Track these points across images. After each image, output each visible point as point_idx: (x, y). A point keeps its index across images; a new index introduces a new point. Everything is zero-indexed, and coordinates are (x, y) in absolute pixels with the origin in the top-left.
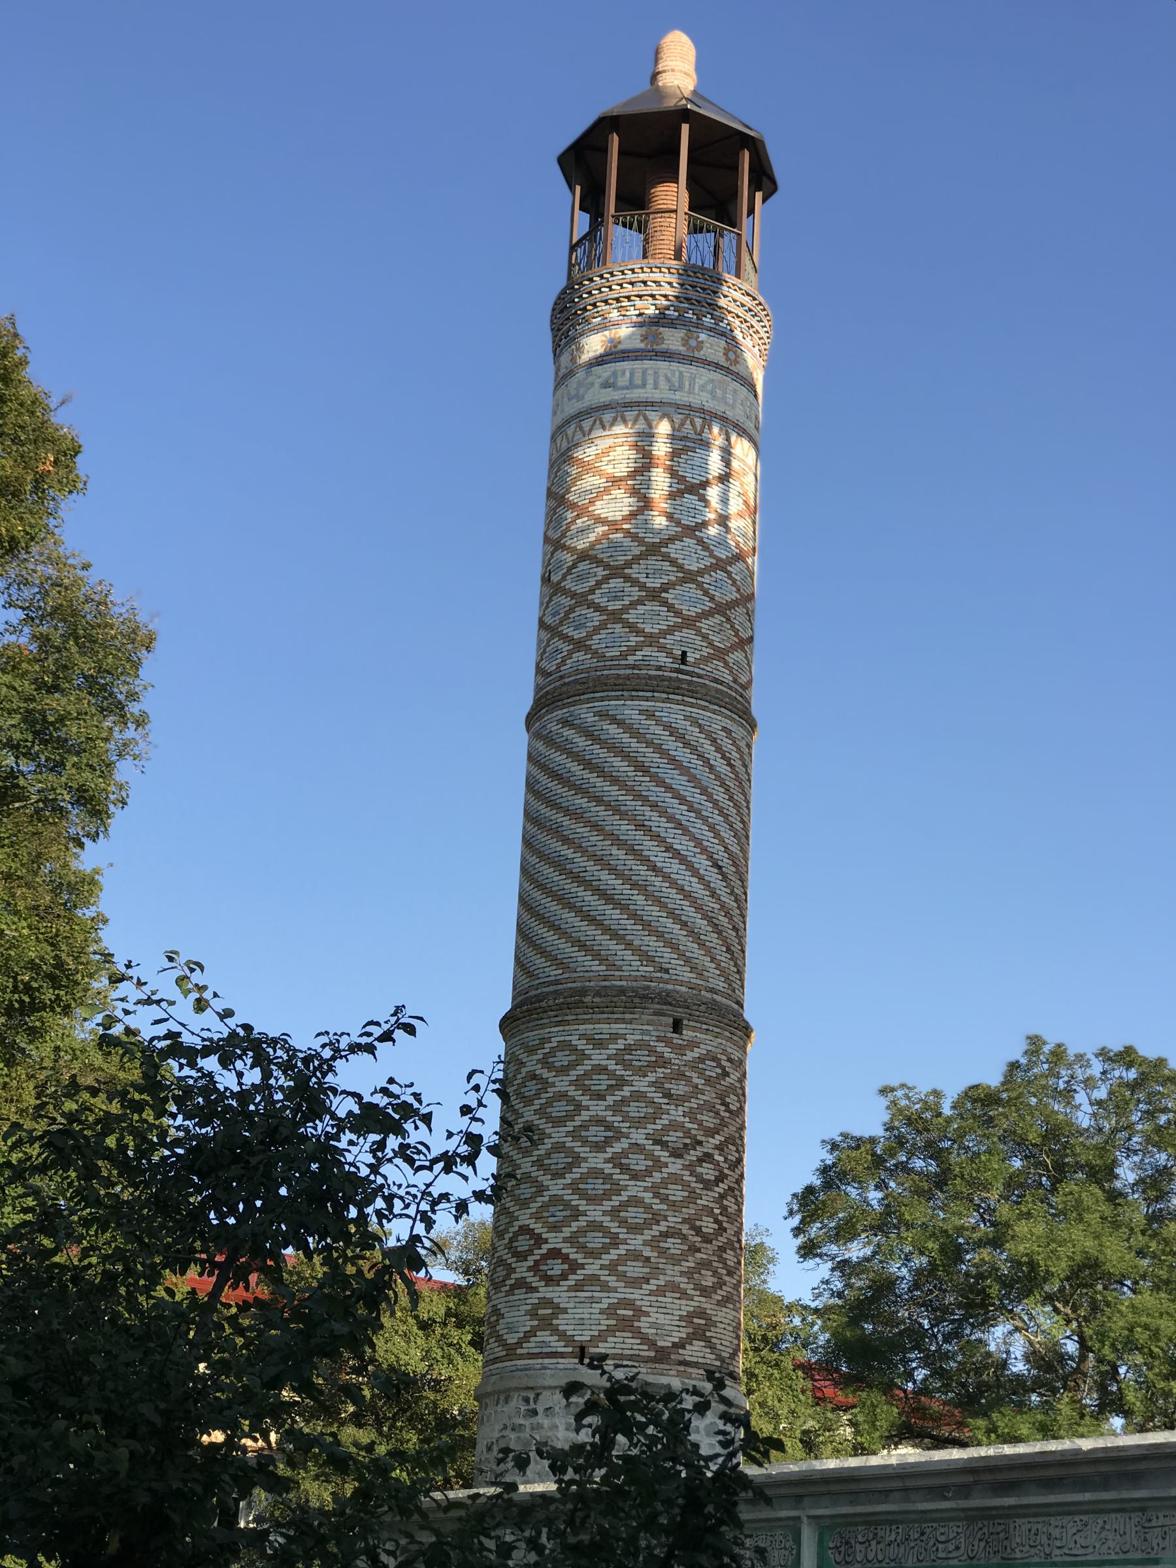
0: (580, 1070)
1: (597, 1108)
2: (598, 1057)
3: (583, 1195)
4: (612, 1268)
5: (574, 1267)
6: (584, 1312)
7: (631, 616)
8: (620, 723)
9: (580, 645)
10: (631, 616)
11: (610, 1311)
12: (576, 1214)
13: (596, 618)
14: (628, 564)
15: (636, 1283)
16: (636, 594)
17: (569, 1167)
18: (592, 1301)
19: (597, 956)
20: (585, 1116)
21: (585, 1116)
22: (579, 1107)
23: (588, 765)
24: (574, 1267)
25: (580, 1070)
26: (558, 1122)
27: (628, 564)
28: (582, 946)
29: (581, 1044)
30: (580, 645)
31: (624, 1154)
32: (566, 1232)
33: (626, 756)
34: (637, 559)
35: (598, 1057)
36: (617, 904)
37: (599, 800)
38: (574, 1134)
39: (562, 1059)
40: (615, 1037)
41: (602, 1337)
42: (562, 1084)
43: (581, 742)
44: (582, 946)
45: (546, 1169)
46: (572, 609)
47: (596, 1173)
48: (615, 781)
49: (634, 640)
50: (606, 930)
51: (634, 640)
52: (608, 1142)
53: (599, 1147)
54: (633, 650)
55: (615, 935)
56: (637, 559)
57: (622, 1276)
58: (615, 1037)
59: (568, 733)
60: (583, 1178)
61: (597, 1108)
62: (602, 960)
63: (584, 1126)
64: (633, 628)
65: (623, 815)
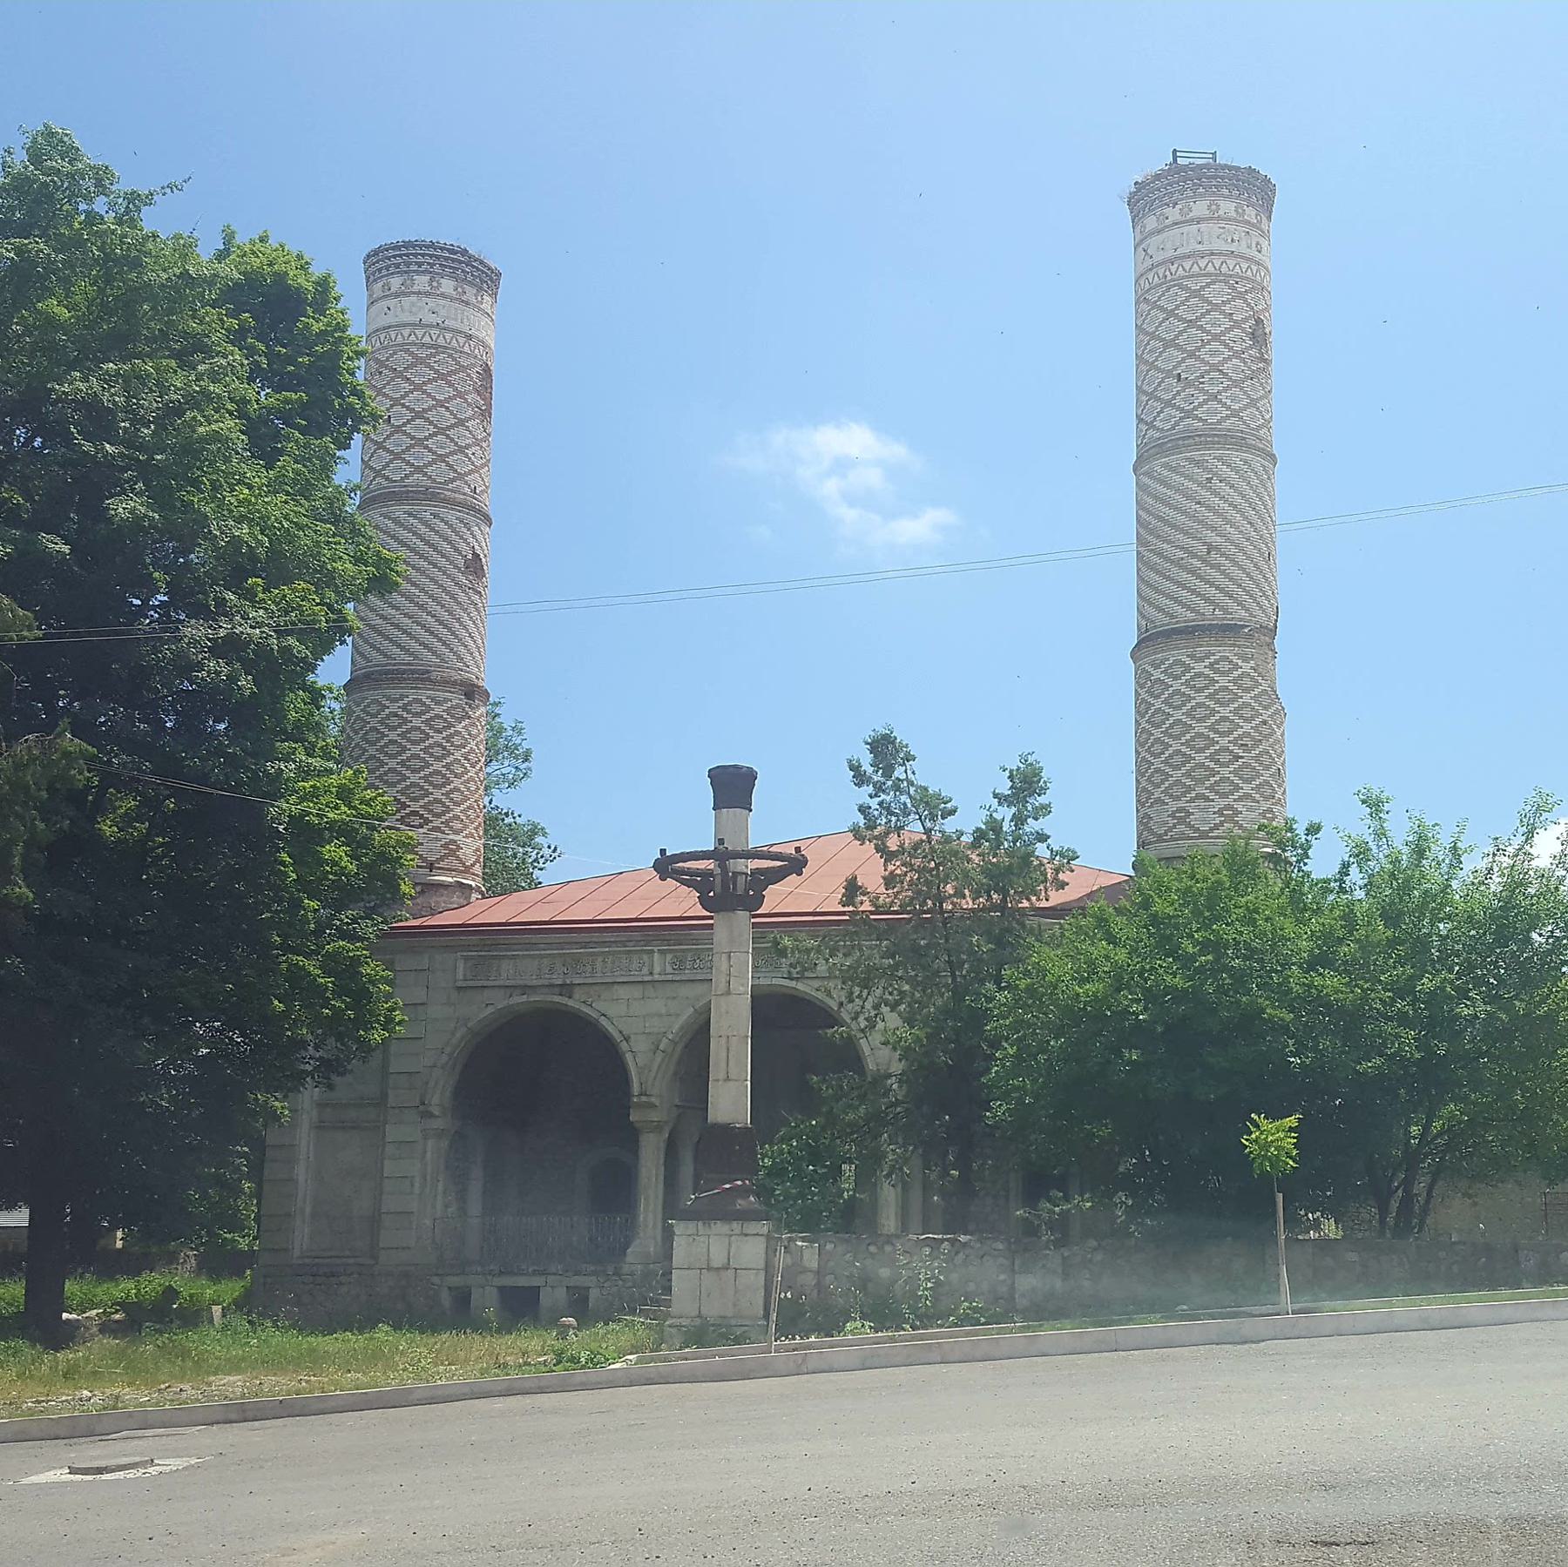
0: (428, 716)
1: (438, 738)
2: (438, 710)
3: (431, 784)
4: (446, 823)
5: (427, 821)
6: (432, 845)
7: (450, 460)
8: (446, 523)
9: (419, 470)
10: (450, 460)
11: (445, 846)
12: (428, 794)
13: (431, 457)
14: (448, 428)
15: (457, 832)
16: (453, 447)
17: (422, 768)
18: (437, 839)
19: (434, 653)
20: (431, 741)
21: (431, 741)
22: (428, 737)
23: (427, 543)
24: (427, 821)
25: (428, 716)
26: (414, 743)
27: (448, 428)
28: (426, 646)
29: (428, 702)
30: (419, 470)
31: (451, 764)
32: (422, 803)
33: (450, 543)
34: (452, 426)
35: (438, 710)
36: (445, 626)
37: (435, 566)
38: (425, 750)
39: (416, 708)
40: (446, 700)
41: (442, 859)
42: (416, 722)
43: (423, 529)
44: (426, 646)
45: (408, 768)
46: (412, 446)
47: (438, 772)
48: (443, 556)
49: (452, 475)
50: (440, 640)
51: (452, 475)
52: (444, 757)
53: (438, 759)
54: (452, 481)
55: (444, 643)
56: (452, 426)
57: (451, 828)
58: (446, 700)
59: (412, 520)
60: (431, 774)
61: (438, 738)
62: (438, 656)
63: (431, 746)
64: (451, 467)
65: (449, 576)
